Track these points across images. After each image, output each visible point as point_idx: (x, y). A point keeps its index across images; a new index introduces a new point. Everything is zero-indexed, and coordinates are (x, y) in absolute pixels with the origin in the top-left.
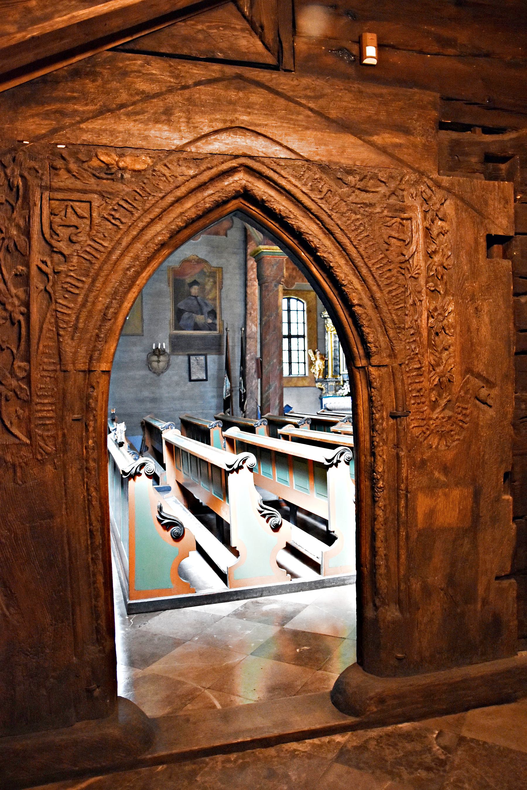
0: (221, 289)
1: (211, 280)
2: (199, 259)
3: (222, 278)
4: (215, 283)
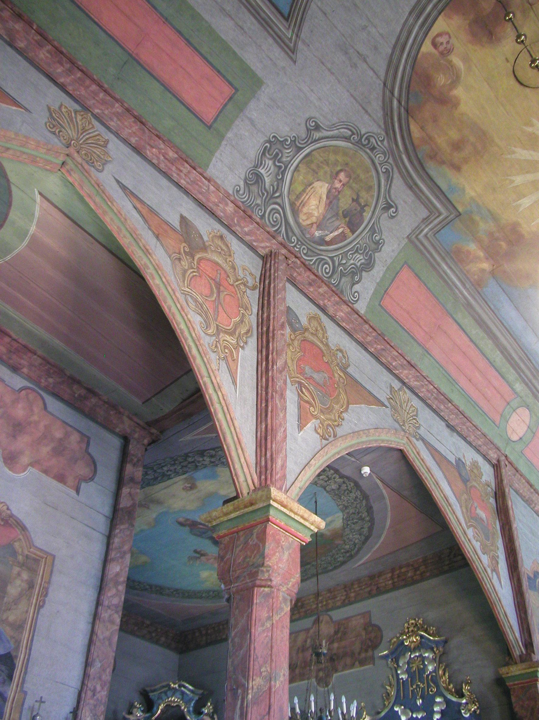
0: (40, 606)
1: (25, 576)
2: (12, 516)
3: (49, 583)
4: (31, 585)
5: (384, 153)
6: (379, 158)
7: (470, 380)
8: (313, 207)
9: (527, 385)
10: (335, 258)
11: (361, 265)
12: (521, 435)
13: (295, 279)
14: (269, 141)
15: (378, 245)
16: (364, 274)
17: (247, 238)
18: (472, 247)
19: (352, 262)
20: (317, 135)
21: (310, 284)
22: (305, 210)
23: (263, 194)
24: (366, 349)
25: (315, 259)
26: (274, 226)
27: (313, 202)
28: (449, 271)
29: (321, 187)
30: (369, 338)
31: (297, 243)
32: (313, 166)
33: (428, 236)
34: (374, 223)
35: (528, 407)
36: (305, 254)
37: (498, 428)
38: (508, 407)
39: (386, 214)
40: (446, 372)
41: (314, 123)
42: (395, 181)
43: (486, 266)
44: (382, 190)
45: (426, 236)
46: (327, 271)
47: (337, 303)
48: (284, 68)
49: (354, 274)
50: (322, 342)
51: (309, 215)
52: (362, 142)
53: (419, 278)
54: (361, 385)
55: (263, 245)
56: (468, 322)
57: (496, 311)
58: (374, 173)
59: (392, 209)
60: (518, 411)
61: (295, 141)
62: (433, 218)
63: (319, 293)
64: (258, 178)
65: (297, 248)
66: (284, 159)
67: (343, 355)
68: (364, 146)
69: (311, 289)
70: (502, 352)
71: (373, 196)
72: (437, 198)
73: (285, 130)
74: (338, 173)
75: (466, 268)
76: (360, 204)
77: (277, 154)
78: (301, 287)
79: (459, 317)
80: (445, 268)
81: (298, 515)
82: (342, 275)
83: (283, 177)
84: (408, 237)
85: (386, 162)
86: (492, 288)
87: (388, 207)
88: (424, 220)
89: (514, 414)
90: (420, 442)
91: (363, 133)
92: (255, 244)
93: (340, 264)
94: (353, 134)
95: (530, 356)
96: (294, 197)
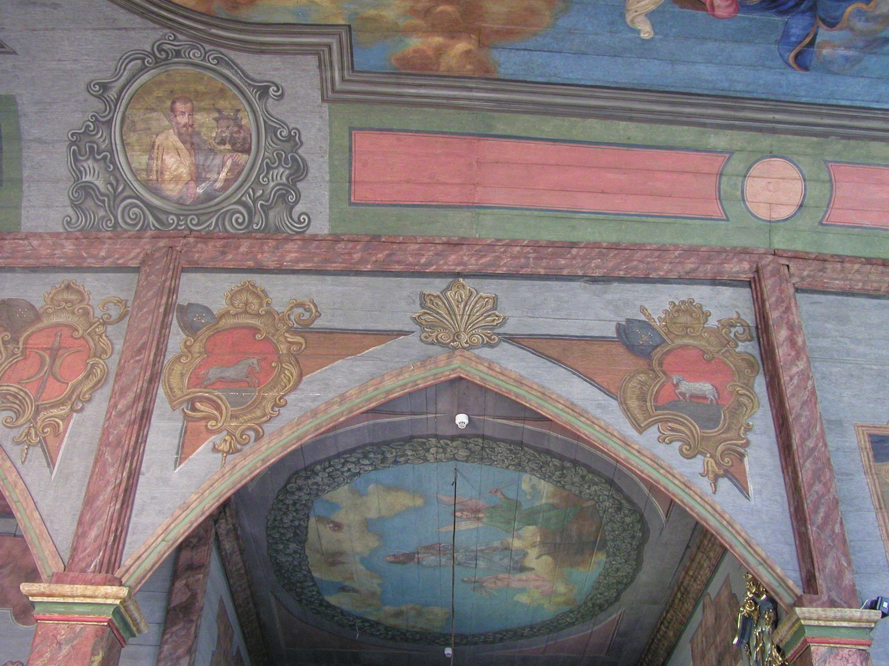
5: (193, 47)
6: (195, 56)
7: (603, 192)
8: (174, 167)
9: (732, 127)
10: (244, 198)
11: (287, 179)
12: (797, 200)
13: (196, 262)
14: (73, 143)
15: (294, 140)
16: (300, 185)
17: (107, 263)
18: (415, 42)
19: (272, 184)
20: (112, 94)
21: (224, 253)
22: (167, 176)
23: (103, 201)
24: (358, 273)
25: (214, 220)
26: (135, 225)
27: (170, 160)
28: (422, 91)
29: (167, 138)
30: (357, 256)
31: (179, 220)
32: (140, 126)
33: (347, 77)
34: (265, 122)
35: (772, 155)
36: (196, 225)
37: (728, 220)
38: (724, 179)
39: (270, 101)
40: (541, 210)
41: (97, 87)
42: (239, 61)
43: (461, 46)
44: (238, 81)
45: (343, 80)
46: (240, 221)
47: (277, 248)
48: (14, 66)
49: (283, 197)
50: (258, 315)
51: (177, 179)
52: (160, 57)
53: (391, 130)
54: (344, 331)
55: (132, 255)
56: (523, 123)
57: (554, 80)
58: (210, 74)
59: (271, 89)
60: (752, 172)
61: (97, 119)
62: (327, 57)
63: (243, 254)
64: (87, 190)
65: (181, 225)
66: (103, 146)
67: (305, 310)
68: (166, 59)
69: (230, 257)
70: (630, 119)
71: (235, 94)
72: (301, 34)
73: (77, 119)
74: (173, 110)
75: (442, 69)
76: (228, 118)
77: (91, 148)
78: (211, 265)
79: (501, 128)
80: (413, 91)
81: (77, 596)
82: (266, 209)
83: (114, 164)
84: (323, 100)
85: (206, 53)
86: (507, 62)
87: (264, 92)
88: (320, 67)
89: (749, 182)
90: (505, 345)
91: (149, 49)
92: (120, 261)
93: (254, 202)
94: (143, 59)
95: (687, 90)
96: (144, 175)
